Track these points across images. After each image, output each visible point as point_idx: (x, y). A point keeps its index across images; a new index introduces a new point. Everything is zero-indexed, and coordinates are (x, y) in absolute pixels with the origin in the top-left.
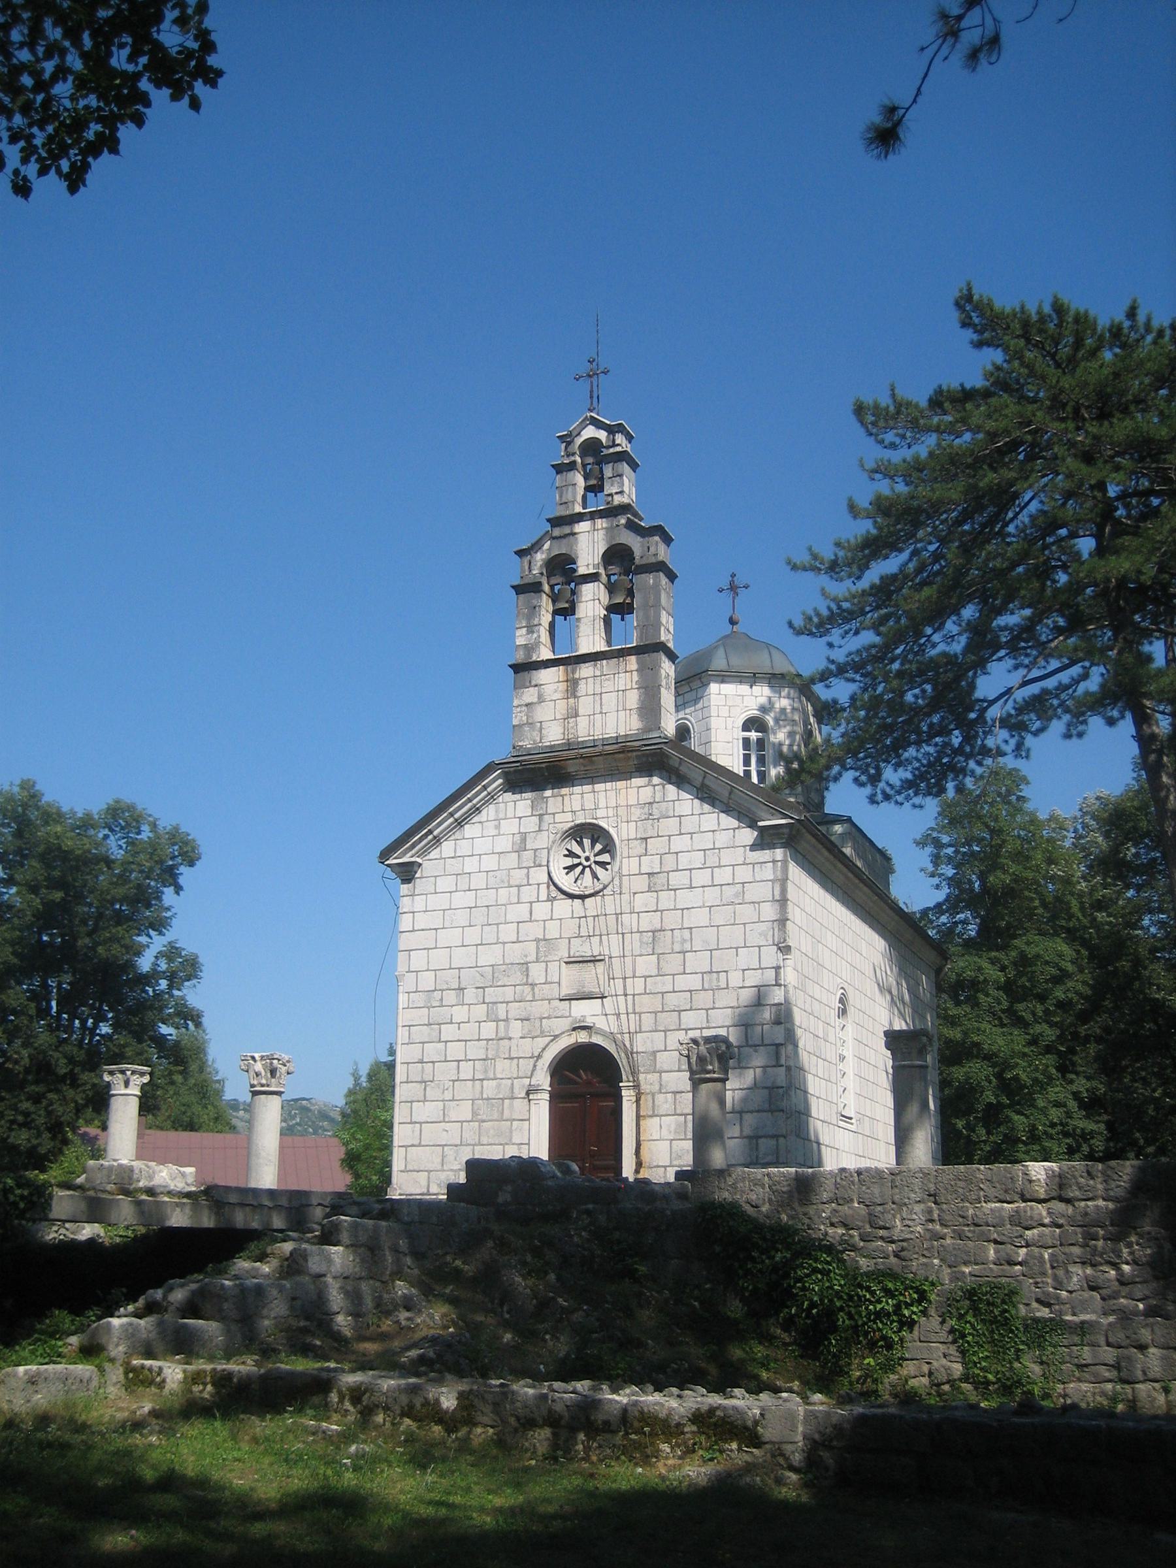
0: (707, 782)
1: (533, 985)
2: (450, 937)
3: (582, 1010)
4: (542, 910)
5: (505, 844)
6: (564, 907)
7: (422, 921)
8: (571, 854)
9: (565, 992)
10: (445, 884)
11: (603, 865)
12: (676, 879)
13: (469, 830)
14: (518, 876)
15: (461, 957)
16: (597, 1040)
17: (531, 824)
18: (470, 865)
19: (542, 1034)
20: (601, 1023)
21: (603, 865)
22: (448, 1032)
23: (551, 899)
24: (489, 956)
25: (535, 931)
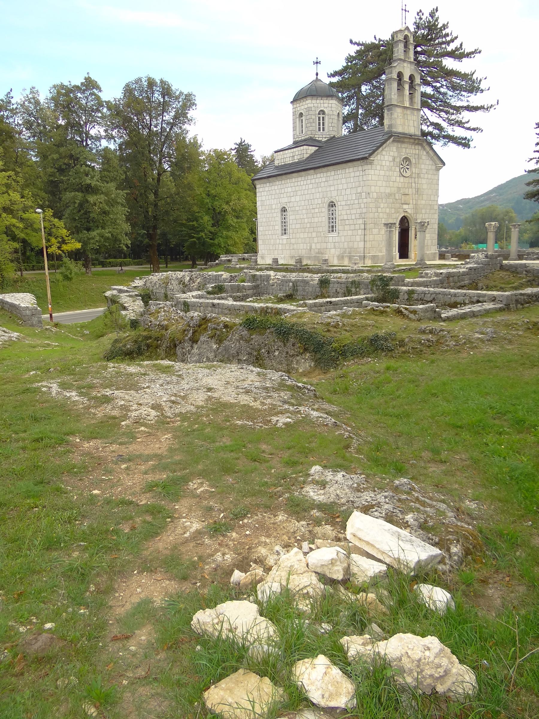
0: (430, 152)
1: (396, 199)
2: (380, 183)
3: (405, 207)
4: (398, 178)
5: (391, 159)
6: (402, 178)
7: (374, 178)
8: (402, 165)
9: (403, 202)
10: (378, 167)
11: (408, 169)
12: (422, 175)
13: (384, 153)
14: (393, 168)
15: (382, 190)
16: (408, 215)
17: (396, 154)
18: (384, 163)
19: (398, 212)
20: (409, 211)
21: (408, 169)
22: (380, 210)
23: (400, 176)
24: (388, 191)
25: (396, 185)
